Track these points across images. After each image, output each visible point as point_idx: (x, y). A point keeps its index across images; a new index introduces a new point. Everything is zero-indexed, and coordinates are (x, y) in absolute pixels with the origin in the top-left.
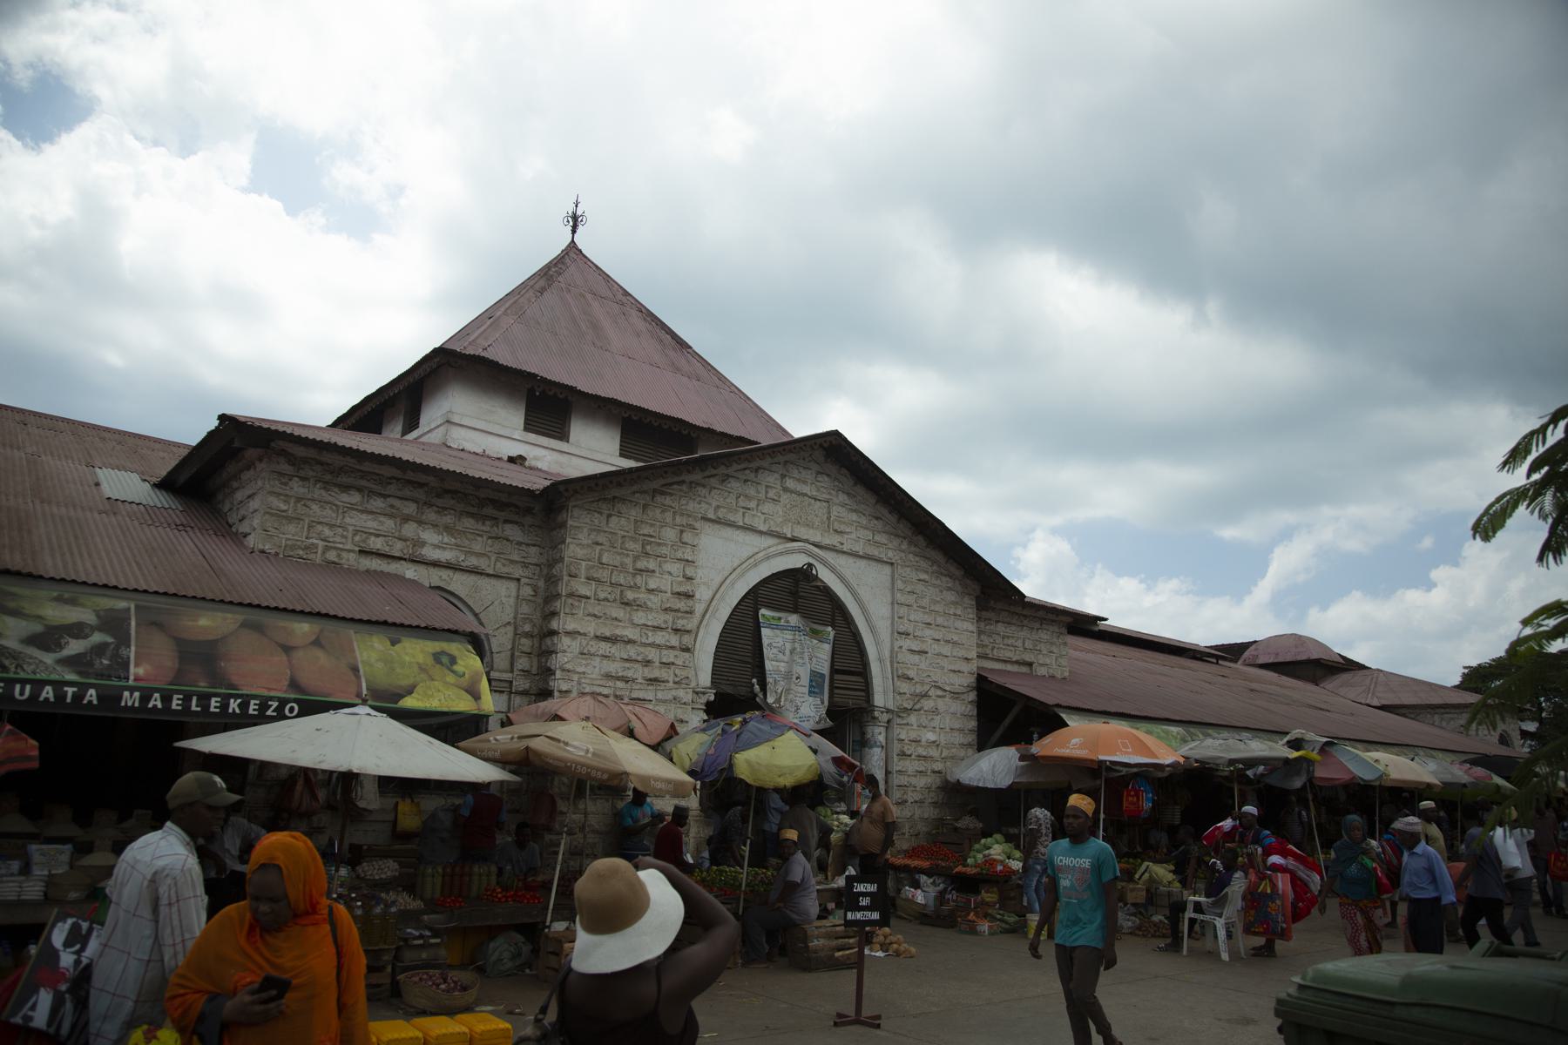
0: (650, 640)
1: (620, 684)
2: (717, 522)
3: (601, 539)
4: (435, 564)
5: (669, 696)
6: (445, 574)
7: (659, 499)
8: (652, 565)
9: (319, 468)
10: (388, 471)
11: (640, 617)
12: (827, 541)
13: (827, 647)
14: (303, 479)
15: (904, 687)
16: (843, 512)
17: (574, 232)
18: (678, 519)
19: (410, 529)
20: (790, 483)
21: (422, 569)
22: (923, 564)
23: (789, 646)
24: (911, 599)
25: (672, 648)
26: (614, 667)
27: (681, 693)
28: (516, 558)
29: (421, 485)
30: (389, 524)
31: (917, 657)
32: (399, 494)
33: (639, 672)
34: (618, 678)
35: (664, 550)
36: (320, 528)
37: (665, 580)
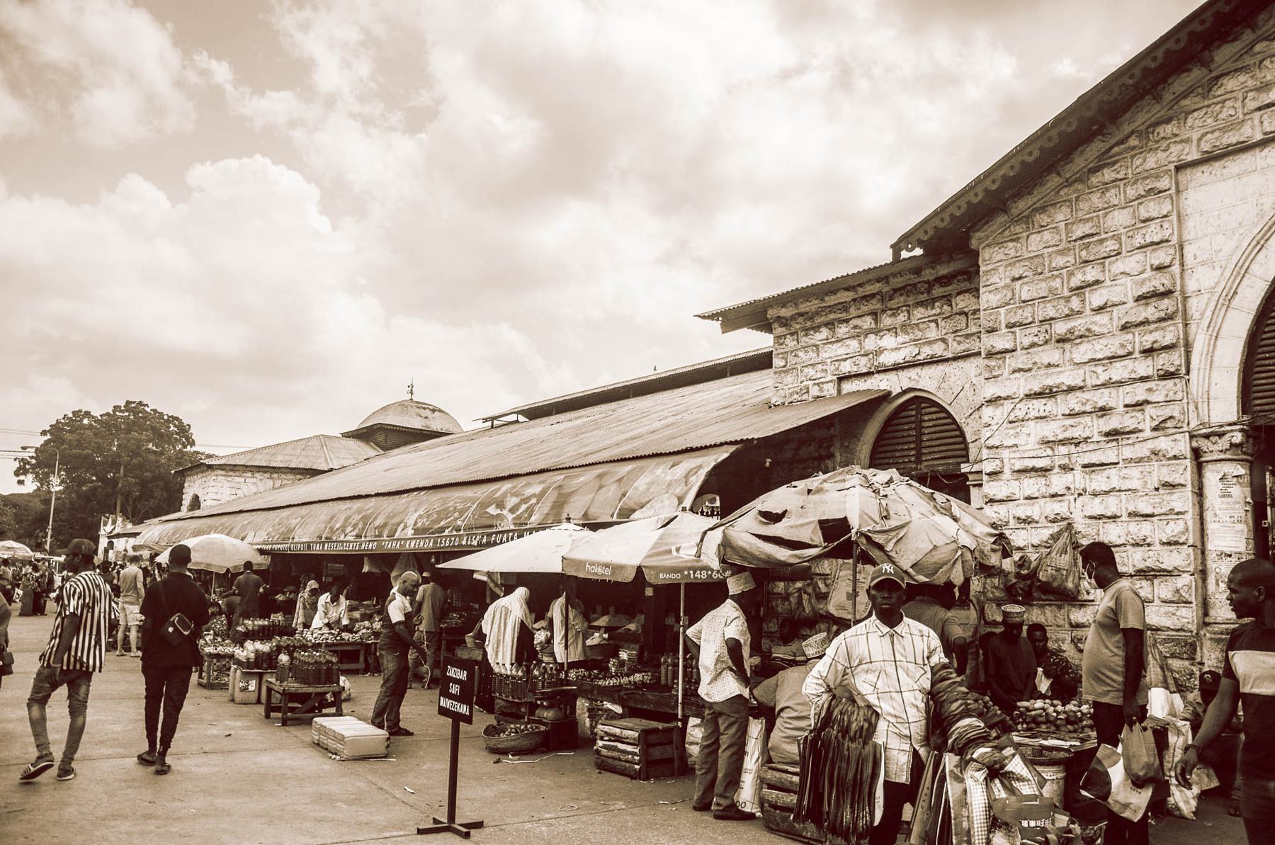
0: (1103, 378)
1: (1063, 450)
2: (1209, 158)
4: (897, 368)
5: (1143, 450)
6: (913, 373)
7: (1094, 180)
8: (1091, 274)
9: (800, 320)
10: (845, 296)
11: (1083, 351)
14: (792, 334)
18: (1131, 192)
19: (871, 343)
21: (892, 376)
25: (1143, 379)
26: (1051, 430)
27: (1163, 443)
29: (873, 296)
30: (854, 344)
34: (1063, 442)
36: (806, 370)
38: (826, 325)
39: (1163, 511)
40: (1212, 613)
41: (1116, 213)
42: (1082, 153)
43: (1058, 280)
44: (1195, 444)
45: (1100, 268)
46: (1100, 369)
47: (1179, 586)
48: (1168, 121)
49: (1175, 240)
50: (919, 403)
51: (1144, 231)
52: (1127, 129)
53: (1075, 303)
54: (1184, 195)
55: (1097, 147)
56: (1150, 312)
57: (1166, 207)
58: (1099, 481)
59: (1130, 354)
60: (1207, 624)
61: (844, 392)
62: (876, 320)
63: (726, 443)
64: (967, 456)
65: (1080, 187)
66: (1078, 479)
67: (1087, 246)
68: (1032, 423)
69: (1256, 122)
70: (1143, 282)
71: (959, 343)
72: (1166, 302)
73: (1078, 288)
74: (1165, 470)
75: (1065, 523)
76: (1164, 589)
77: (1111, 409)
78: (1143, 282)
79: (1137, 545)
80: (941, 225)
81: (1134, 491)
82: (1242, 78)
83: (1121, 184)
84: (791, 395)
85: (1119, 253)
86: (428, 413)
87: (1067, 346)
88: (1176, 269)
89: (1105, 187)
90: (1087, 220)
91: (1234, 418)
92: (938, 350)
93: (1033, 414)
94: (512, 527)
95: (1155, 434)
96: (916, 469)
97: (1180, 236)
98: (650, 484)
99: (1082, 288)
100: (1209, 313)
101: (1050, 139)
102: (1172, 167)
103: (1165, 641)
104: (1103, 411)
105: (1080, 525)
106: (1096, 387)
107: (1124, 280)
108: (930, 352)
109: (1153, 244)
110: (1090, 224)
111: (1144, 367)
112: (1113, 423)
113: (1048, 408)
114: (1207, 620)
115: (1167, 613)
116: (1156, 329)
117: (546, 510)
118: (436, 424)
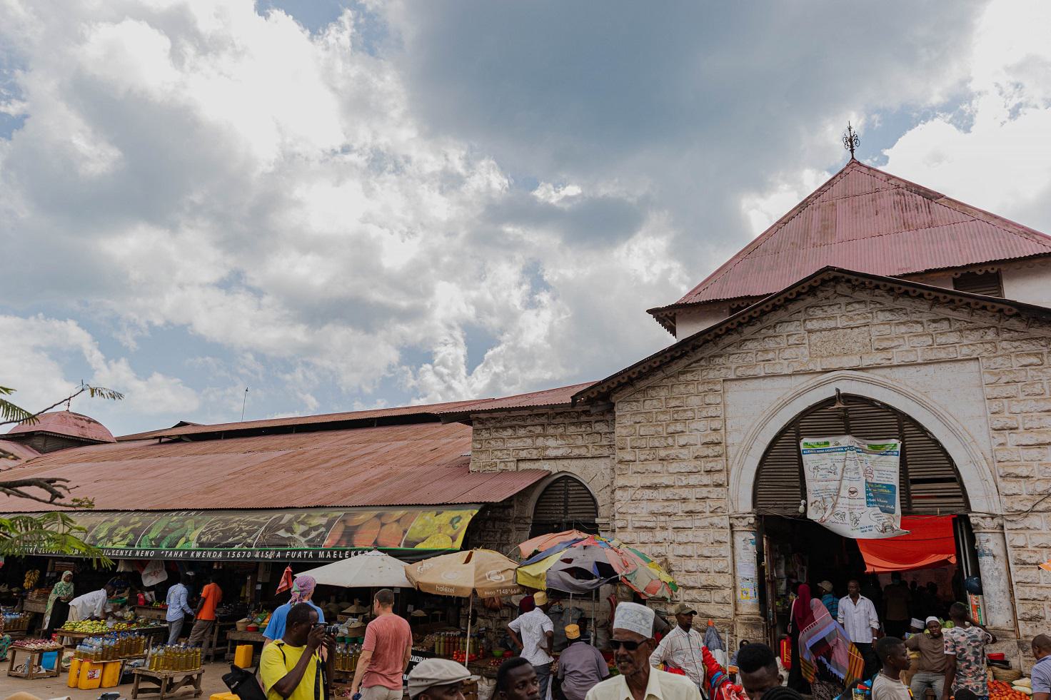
0: (685, 483)
1: (662, 518)
3: (638, 418)
4: (556, 458)
5: (706, 523)
6: (566, 462)
7: (682, 378)
8: (679, 427)
9: (493, 421)
10: (526, 413)
11: (674, 467)
12: (866, 362)
13: (895, 460)
14: (486, 429)
15: (1010, 487)
16: (886, 330)
17: (852, 151)
18: (701, 388)
20: (809, 325)
21: (552, 462)
22: (1027, 347)
23: (840, 466)
24: (1011, 390)
25: (705, 486)
26: (655, 507)
27: (716, 520)
28: (605, 443)
29: (543, 415)
30: (529, 441)
31: (1034, 453)
32: (533, 423)
33: (679, 508)
34: (662, 514)
35: (690, 414)
36: (496, 453)
37: (697, 433)
38: (511, 427)
39: (715, 555)
40: (739, 609)
41: (693, 397)
42: (676, 364)
43: (661, 427)
44: (731, 522)
45: (683, 425)
46: (683, 478)
47: (725, 595)
48: (721, 356)
49: (722, 417)
50: (567, 479)
51: (707, 409)
52: (700, 356)
53: (670, 441)
54: (726, 395)
55: (684, 362)
56: (710, 451)
57: (719, 400)
58: (682, 537)
59: (699, 472)
60: (737, 615)
61: (520, 469)
62: (544, 429)
63: (473, 503)
64: (597, 513)
65: (674, 380)
66: (670, 534)
67: (677, 412)
68: (645, 502)
69: (762, 367)
70: (707, 436)
71: (596, 450)
72: (718, 448)
73: (671, 433)
74: (716, 533)
75: (663, 558)
76: (717, 596)
77: (688, 499)
78: (707, 436)
79: (703, 572)
80: (602, 391)
81: (701, 543)
82: (756, 344)
83: (696, 383)
84: (485, 466)
85: (694, 419)
86: (84, 423)
87: (665, 463)
88: (723, 431)
89: (687, 383)
90: (678, 398)
91: (750, 511)
92: (583, 452)
93: (646, 497)
94: (307, 547)
95: (712, 515)
96: (564, 518)
97: (725, 415)
98: (424, 526)
99: (674, 433)
100: (738, 456)
101: (666, 357)
102: (721, 380)
103: (719, 624)
104: (684, 500)
105: (671, 560)
106: (681, 487)
107: (696, 433)
109: (711, 417)
110: (679, 401)
111: (706, 479)
112: (690, 507)
113: (654, 495)
114: (737, 613)
115: (718, 609)
116: (712, 461)
117: (337, 537)
118: (91, 434)
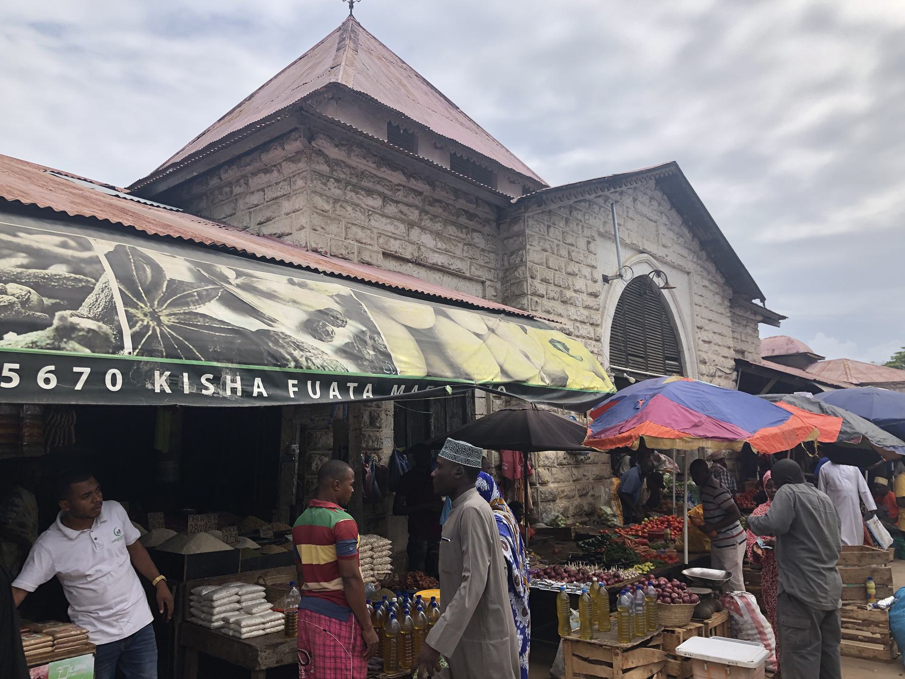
9: (346, 170)
17: (351, 7)
19: (415, 233)
25: (591, 339)
36: (354, 229)
108: (460, 267)
